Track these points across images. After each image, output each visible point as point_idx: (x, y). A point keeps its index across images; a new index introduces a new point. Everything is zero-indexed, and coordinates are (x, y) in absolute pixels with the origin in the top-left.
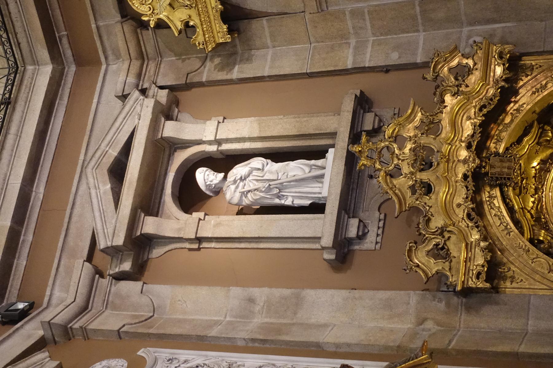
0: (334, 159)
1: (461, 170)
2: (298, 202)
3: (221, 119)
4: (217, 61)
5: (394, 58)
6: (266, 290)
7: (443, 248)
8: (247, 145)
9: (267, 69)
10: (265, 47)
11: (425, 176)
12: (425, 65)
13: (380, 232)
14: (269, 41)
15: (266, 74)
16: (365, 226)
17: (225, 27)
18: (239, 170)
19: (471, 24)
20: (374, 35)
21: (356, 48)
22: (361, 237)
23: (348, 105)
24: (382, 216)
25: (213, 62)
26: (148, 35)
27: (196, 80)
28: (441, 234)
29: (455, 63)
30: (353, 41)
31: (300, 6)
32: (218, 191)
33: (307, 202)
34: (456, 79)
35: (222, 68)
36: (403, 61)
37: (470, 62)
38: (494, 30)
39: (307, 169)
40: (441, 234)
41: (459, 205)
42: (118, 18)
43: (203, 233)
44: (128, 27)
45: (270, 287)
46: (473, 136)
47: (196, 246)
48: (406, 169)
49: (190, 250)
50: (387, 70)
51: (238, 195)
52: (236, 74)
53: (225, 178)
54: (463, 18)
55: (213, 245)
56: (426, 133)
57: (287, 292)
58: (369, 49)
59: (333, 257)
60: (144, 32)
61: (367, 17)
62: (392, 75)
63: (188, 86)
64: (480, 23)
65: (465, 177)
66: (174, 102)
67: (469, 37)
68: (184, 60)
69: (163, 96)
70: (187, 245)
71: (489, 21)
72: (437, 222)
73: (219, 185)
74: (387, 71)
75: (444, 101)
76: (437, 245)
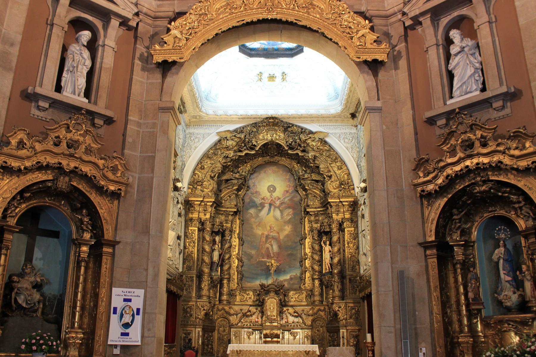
0: (82, 101)
1: (64, 163)
2: (63, 79)
3: (116, 50)
4: (146, 54)
5: (129, 139)
6: (17, 54)
7: (23, 147)
8: (99, 60)
9: (137, 77)
10: (148, 79)
11: (64, 144)
12: (123, 154)
13: (40, 118)
14: (150, 81)
15: (134, 77)
16: (44, 111)
17: (160, 61)
18: (86, 54)
19: (139, 178)
20: (143, 132)
21: (138, 122)
22: (38, 108)
23: (109, 113)
24: (48, 120)
25: (146, 52)
26: (165, 23)
27: (138, 42)
28: (31, 147)
29: (120, 167)
30: (141, 121)
31: (164, 99)
32: (77, 40)
33: (63, 84)
34: (111, 167)
35: (142, 55)
36: (127, 143)
37: (119, 175)
38: (134, 189)
39: (80, 87)
40: (31, 147)
41: (45, 158)
42: (177, 11)
43: (55, 27)
44: (171, 14)
45: (18, 56)
46: (81, 170)
47: (49, 22)
48: (69, 136)
49: (47, 19)
50: (124, 135)
51: (74, 50)
52: (137, 62)
53: (84, 46)
54: (142, 175)
55: (48, 32)
56: (86, 149)
57: (14, 64)
58: (136, 128)
59: (29, 91)
60: (167, 22)
61: (152, 130)
62: (122, 137)
63: (136, 37)
64: (139, 182)
65: (60, 164)
66: (129, 28)
67: (132, 176)
68: (149, 38)
69: (133, 24)
70: (50, 18)
71: (138, 186)
72: (38, 147)
73: (80, 42)
74: (123, 135)
75: (101, 159)
76: (25, 144)
